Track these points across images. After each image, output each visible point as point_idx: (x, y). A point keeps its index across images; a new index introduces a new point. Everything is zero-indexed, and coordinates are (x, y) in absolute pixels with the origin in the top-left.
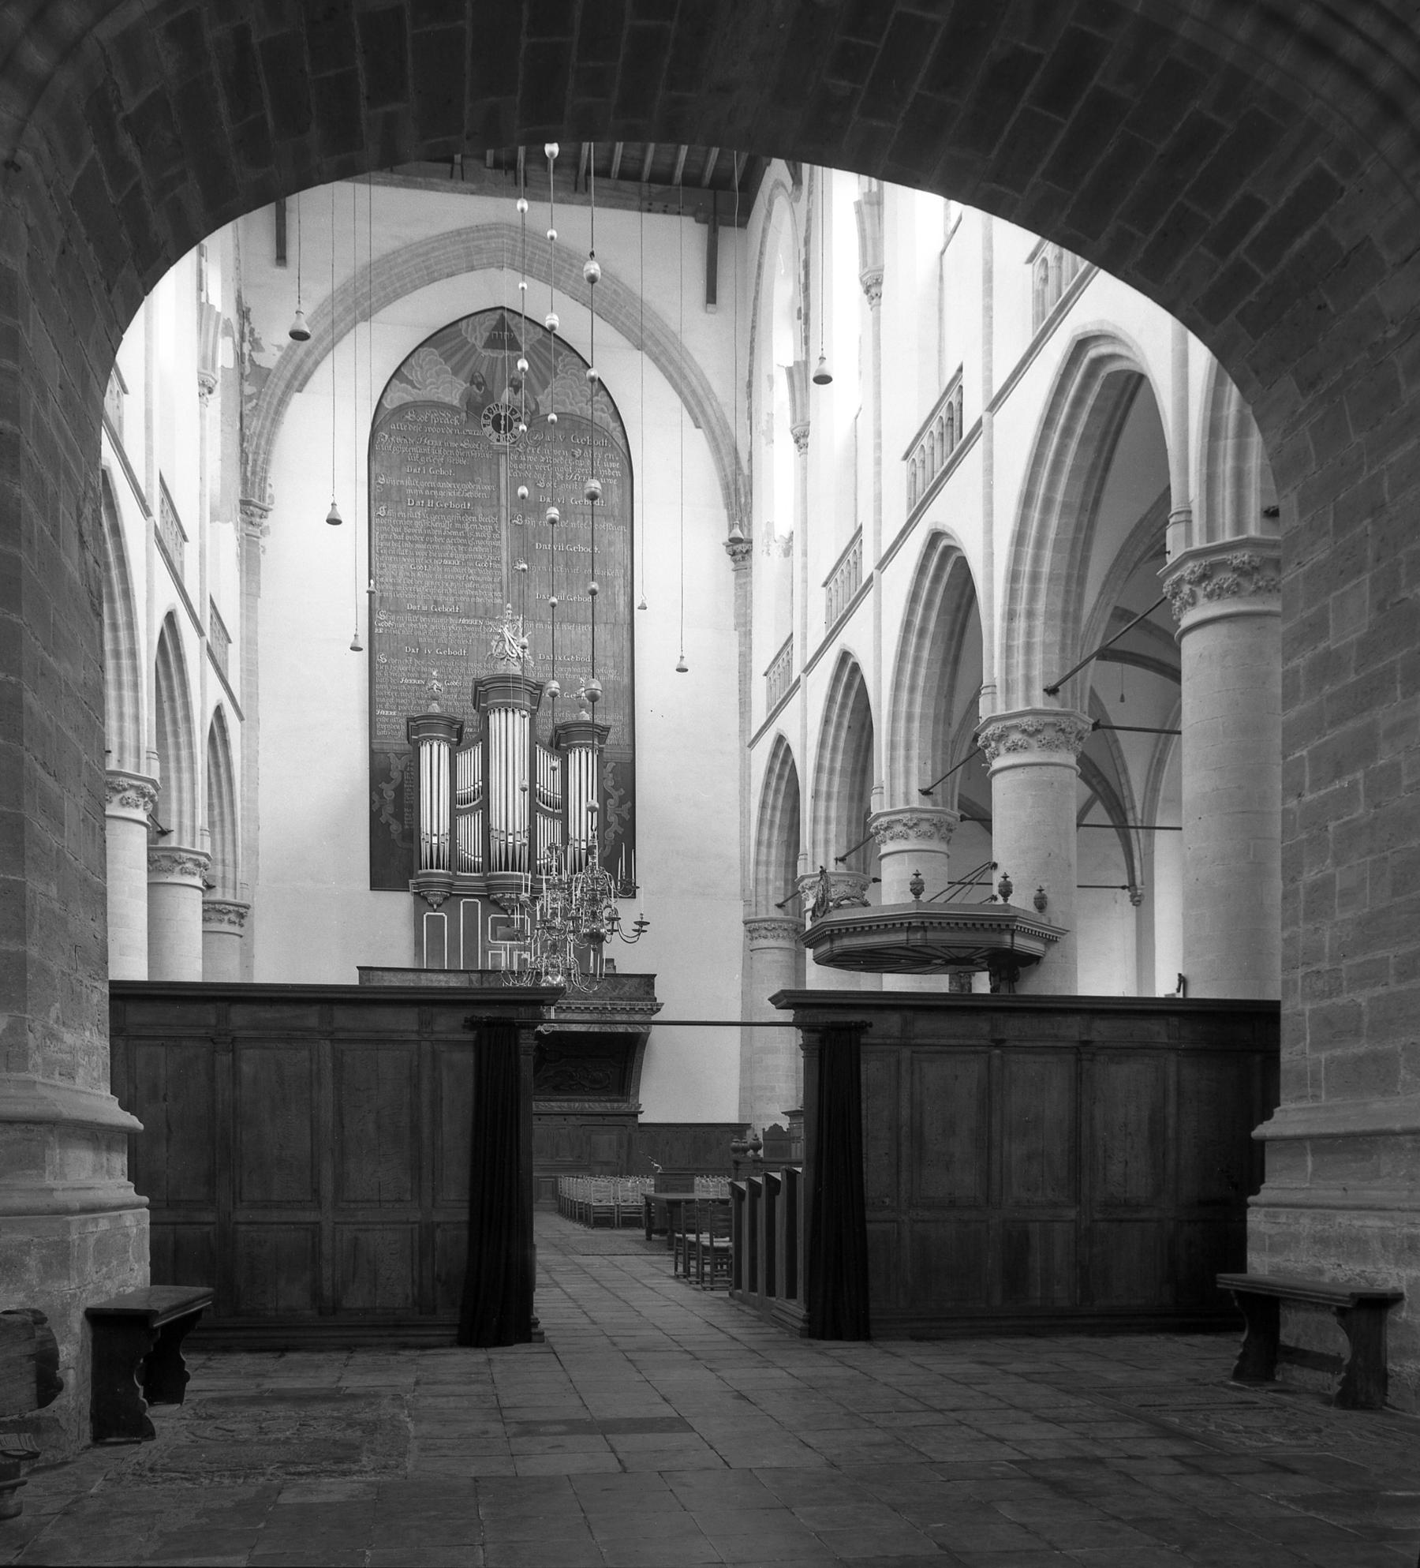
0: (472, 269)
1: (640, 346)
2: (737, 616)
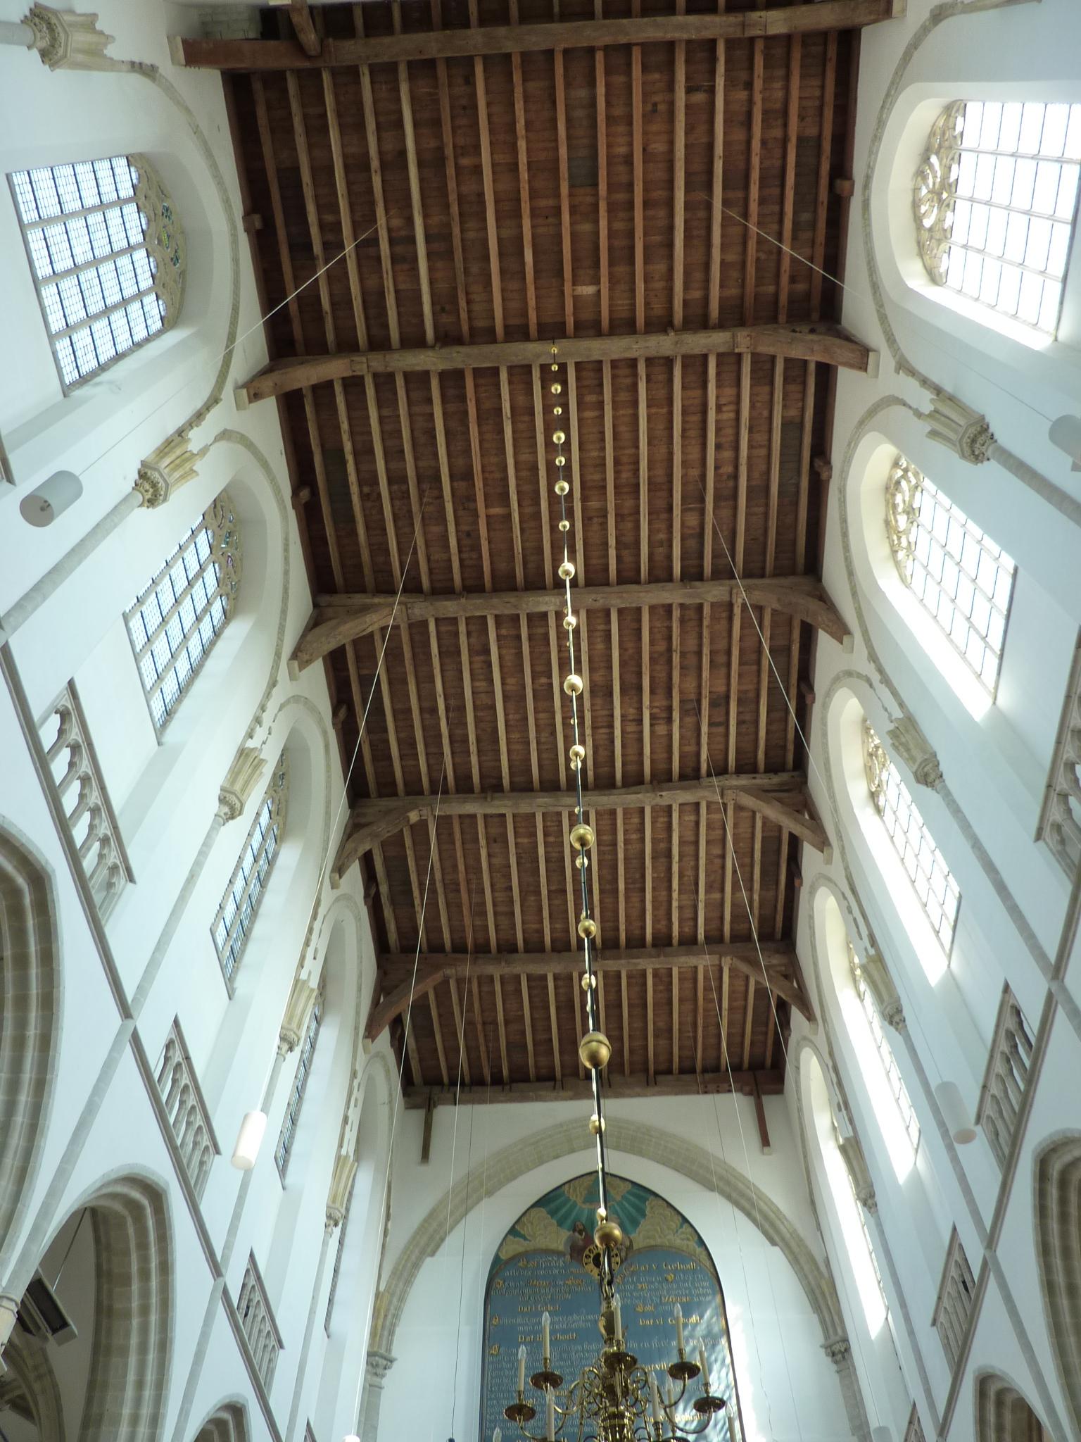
0: (572, 1151)
1: (711, 1187)
2: (851, 1419)
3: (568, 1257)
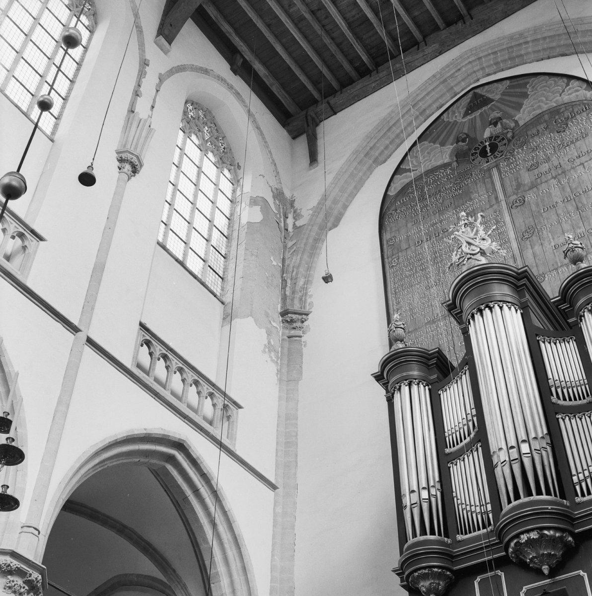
3: (455, 163)
